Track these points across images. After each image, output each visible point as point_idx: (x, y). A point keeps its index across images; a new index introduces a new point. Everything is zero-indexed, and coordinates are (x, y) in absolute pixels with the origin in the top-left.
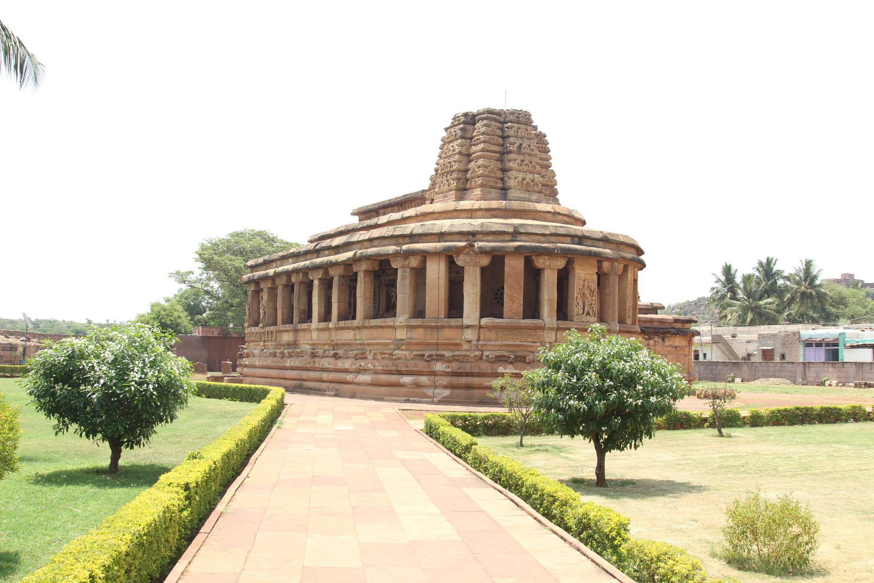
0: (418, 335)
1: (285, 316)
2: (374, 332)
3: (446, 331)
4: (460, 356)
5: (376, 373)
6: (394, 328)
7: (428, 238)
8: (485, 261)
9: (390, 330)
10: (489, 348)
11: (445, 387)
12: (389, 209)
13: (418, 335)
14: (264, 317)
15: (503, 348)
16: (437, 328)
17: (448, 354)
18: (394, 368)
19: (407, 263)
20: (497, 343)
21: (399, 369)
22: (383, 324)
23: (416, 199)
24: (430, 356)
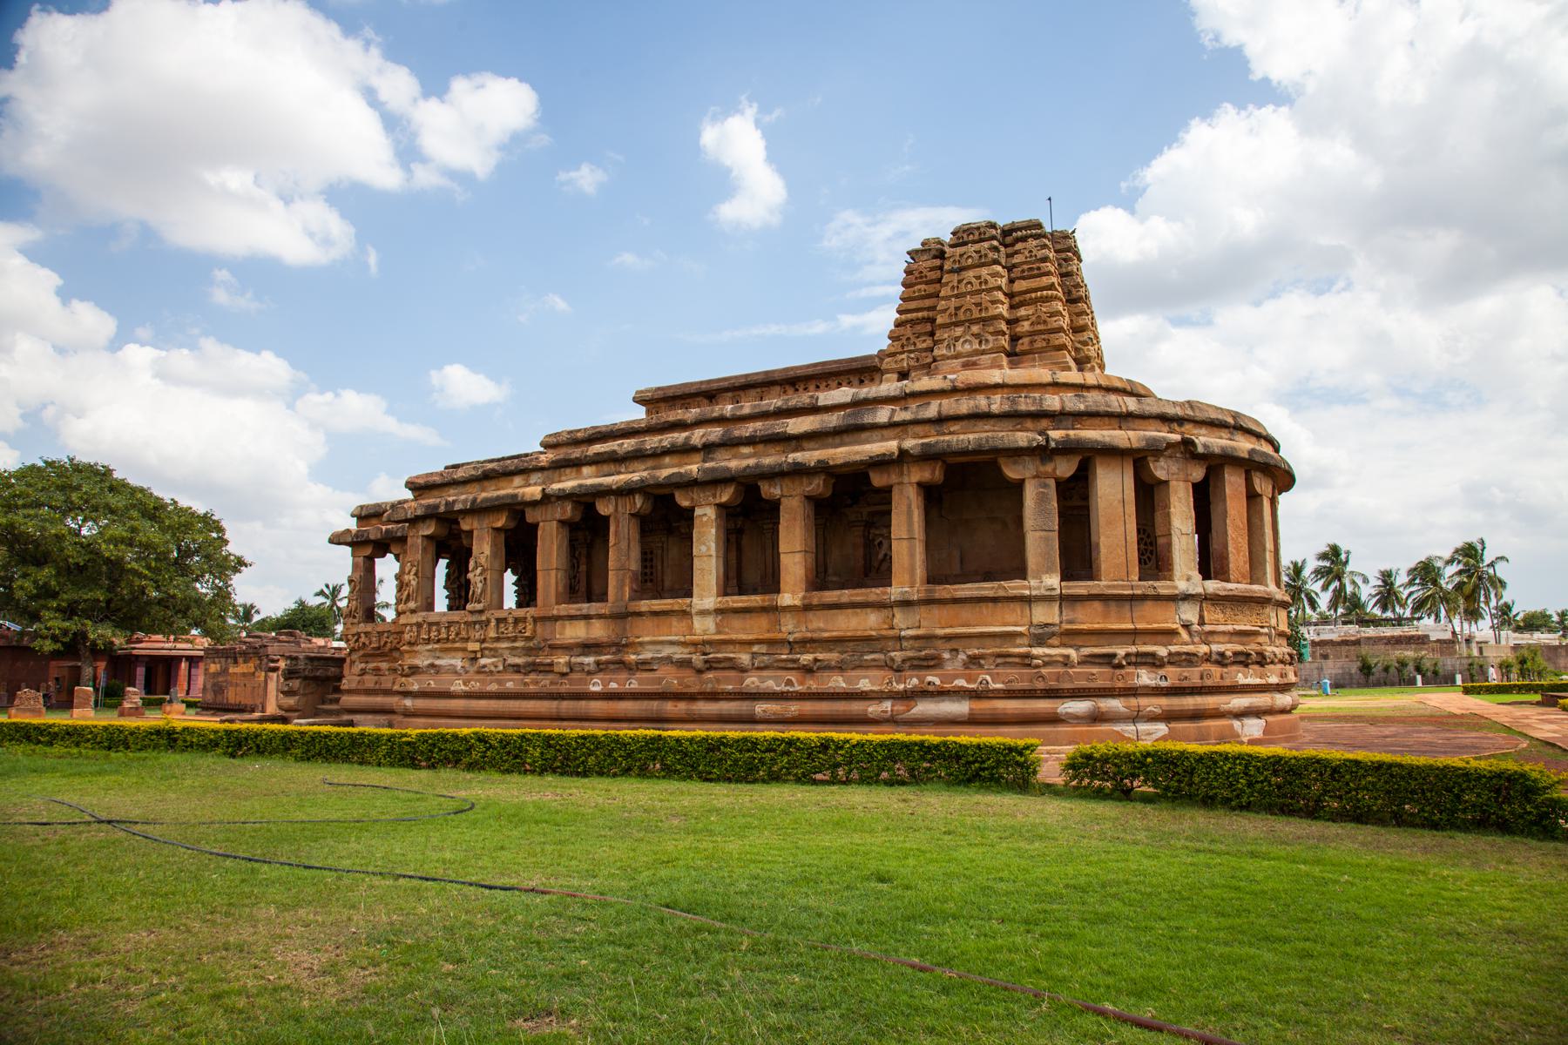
0: (1088, 618)
1: (561, 589)
2: (966, 612)
3: (1149, 603)
4: (1178, 654)
5: (974, 695)
6: (1028, 600)
7: (1097, 421)
8: (1198, 474)
9: (1017, 606)
10: (1217, 638)
11: (1153, 718)
12: (753, 392)
13: (1088, 618)
14: (483, 591)
15: (1235, 638)
16: (1132, 598)
17: (1162, 651)
18: (1040, 685)
19: (1049, 468)
20: (1230, 628)
21: (1053, 684)
22: (1001, 593)
23: (861, 370)
24: (1128, 655)
